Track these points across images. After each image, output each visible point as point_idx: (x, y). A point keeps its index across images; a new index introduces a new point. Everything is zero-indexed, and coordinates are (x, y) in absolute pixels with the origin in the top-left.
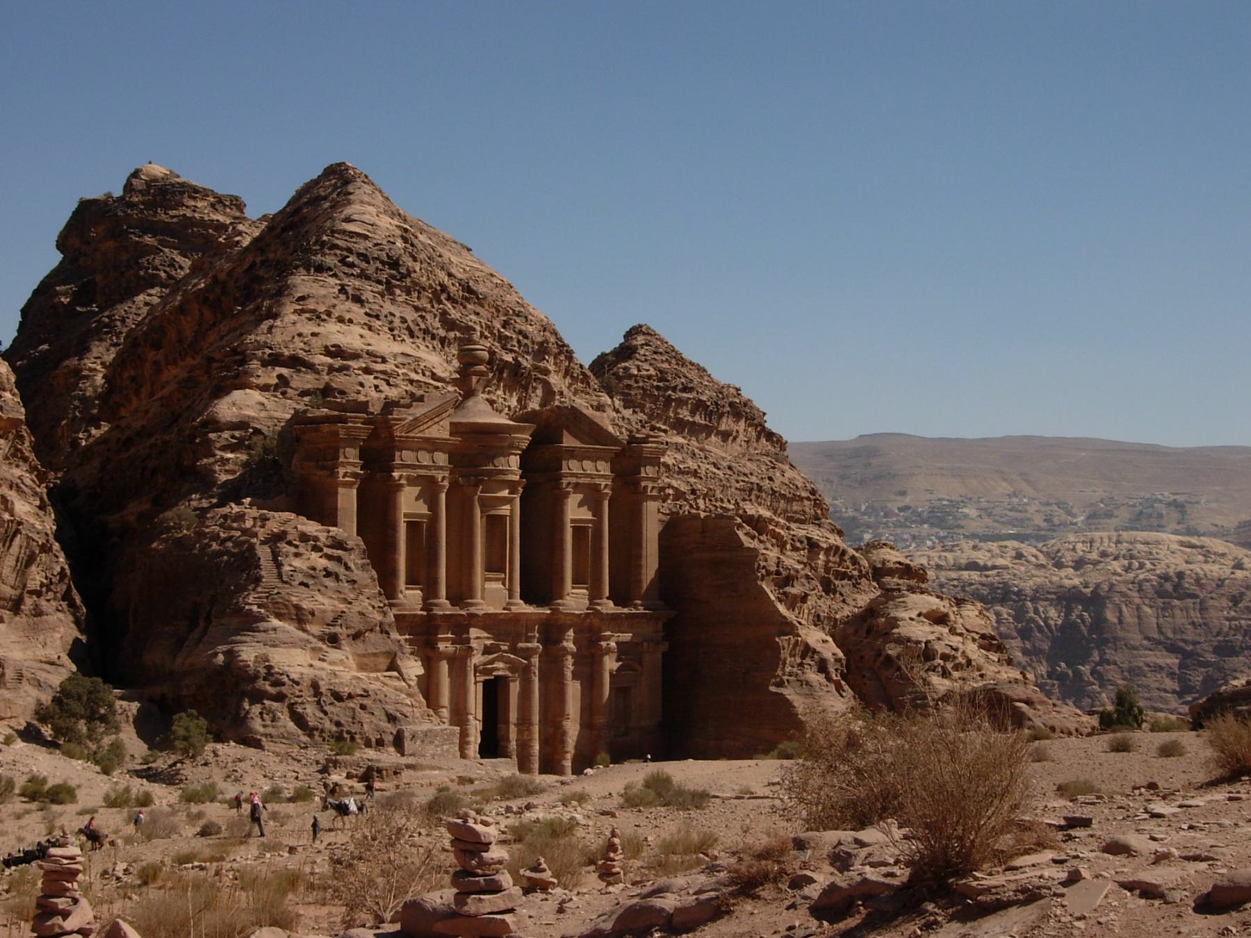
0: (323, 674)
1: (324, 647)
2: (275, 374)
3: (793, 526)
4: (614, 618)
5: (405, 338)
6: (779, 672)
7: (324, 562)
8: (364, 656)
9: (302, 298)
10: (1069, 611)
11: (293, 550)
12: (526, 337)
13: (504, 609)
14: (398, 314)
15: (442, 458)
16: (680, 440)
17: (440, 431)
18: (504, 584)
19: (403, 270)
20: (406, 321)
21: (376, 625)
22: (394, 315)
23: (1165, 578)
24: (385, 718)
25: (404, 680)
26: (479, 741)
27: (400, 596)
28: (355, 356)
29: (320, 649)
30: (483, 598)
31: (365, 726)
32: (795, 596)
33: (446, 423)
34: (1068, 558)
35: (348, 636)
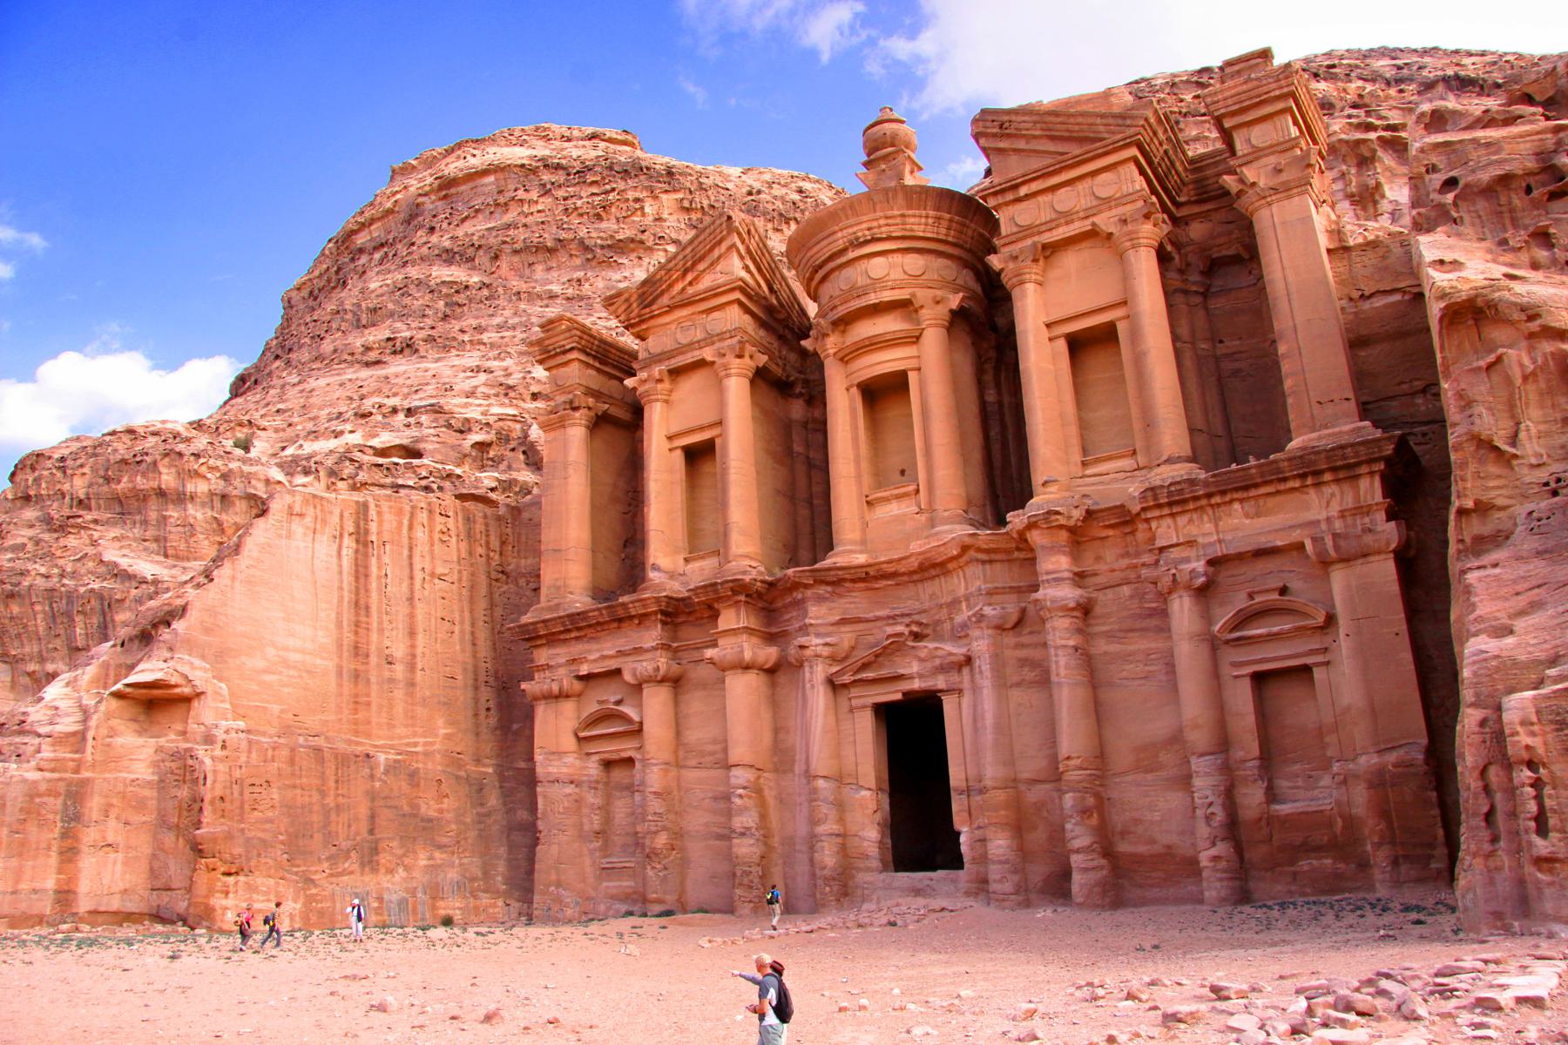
4: (1176, 500)
27: (652, 575)
30: (863, 542)
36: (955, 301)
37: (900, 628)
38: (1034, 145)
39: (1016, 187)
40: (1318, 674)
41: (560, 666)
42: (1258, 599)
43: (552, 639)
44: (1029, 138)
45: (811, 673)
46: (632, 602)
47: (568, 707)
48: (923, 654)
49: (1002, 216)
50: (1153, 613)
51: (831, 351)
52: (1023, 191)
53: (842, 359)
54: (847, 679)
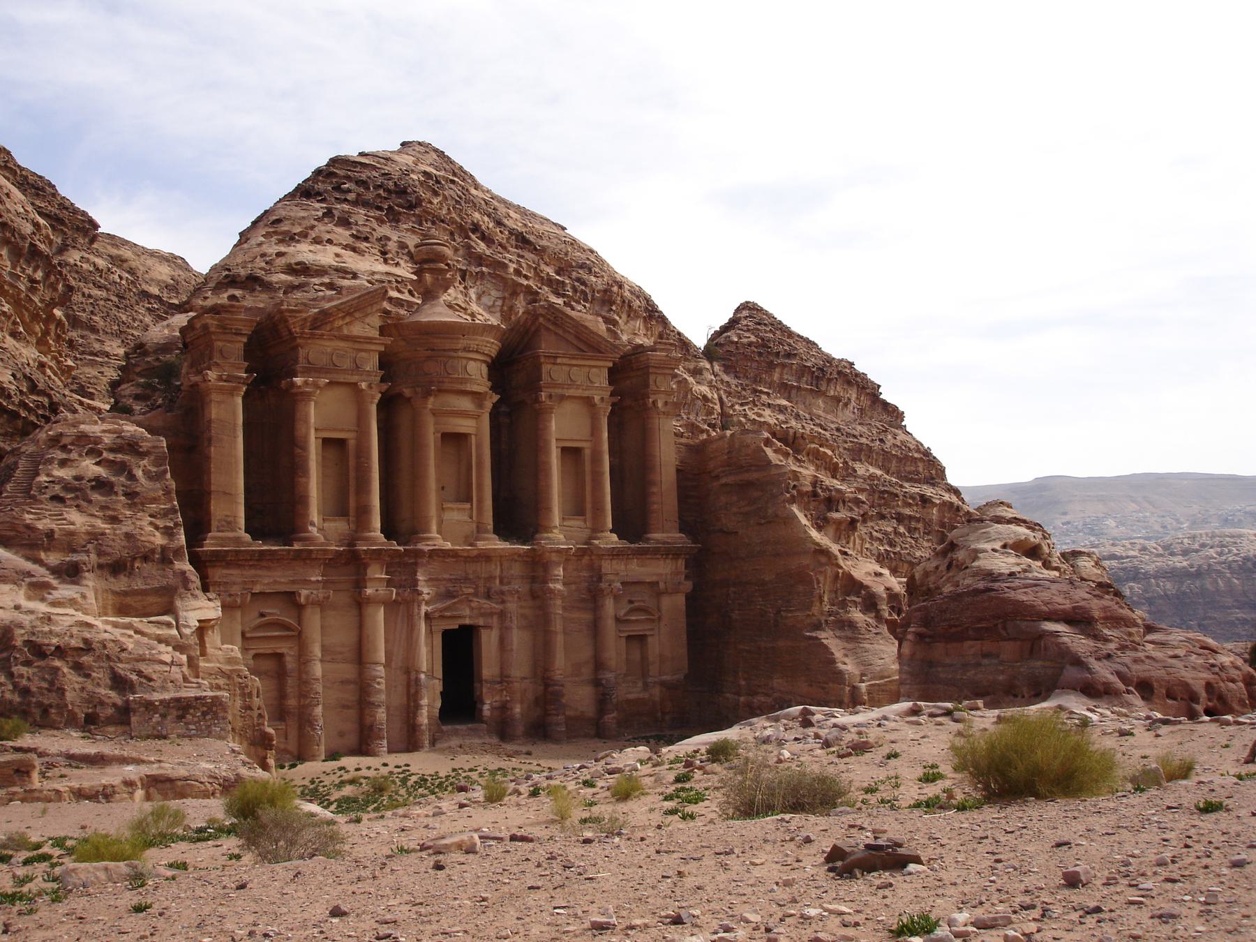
0: (26, 619)
1: (55, 582)
2: (226, 295)
3: (906, 485)
4: (615, 554)
5: (402, 262)
6: (815, 610)
7: (101, 471)
8: (125, 594)
9: (279, 221)
10: (1182, 583)
11: (64, 456)
12: (583, 283)
13: (471, 545)
14: (395, 238)
15: (371, 363)
16: (784, 402)
17: (367, 327)
18: (471, 518)
19: (412, 199)
20: (407, 247)
21: (153, 551)
22: (389, 239)
23: (1246, 559)
24: (108, 682)
25: (178, 628)
26: (438, 704)
27: (310, 528)
28: (321, 271)
29: (46, 586)
30: (439, 532)
31: (68, 694)
32: (839, 523)
33: (376, 321)
34: (1177, 549)
35: (100, 566)
36: (496, 398)
37: (471, 591)
38: (566, 336)
39: (556, 357)
40: (650, 639)
41: (234, 584)
42: (636, 604)
43: (229, 565)
44: (565, 331)
45: (419, 610)
46: (318, 550)
47: (238, 614)
48: (473, 605)
49: (546, 368)
50: (583, 600)
51: (430, 406)
52: (559, 361)
53: (434, 414)
54: (437, 615)
